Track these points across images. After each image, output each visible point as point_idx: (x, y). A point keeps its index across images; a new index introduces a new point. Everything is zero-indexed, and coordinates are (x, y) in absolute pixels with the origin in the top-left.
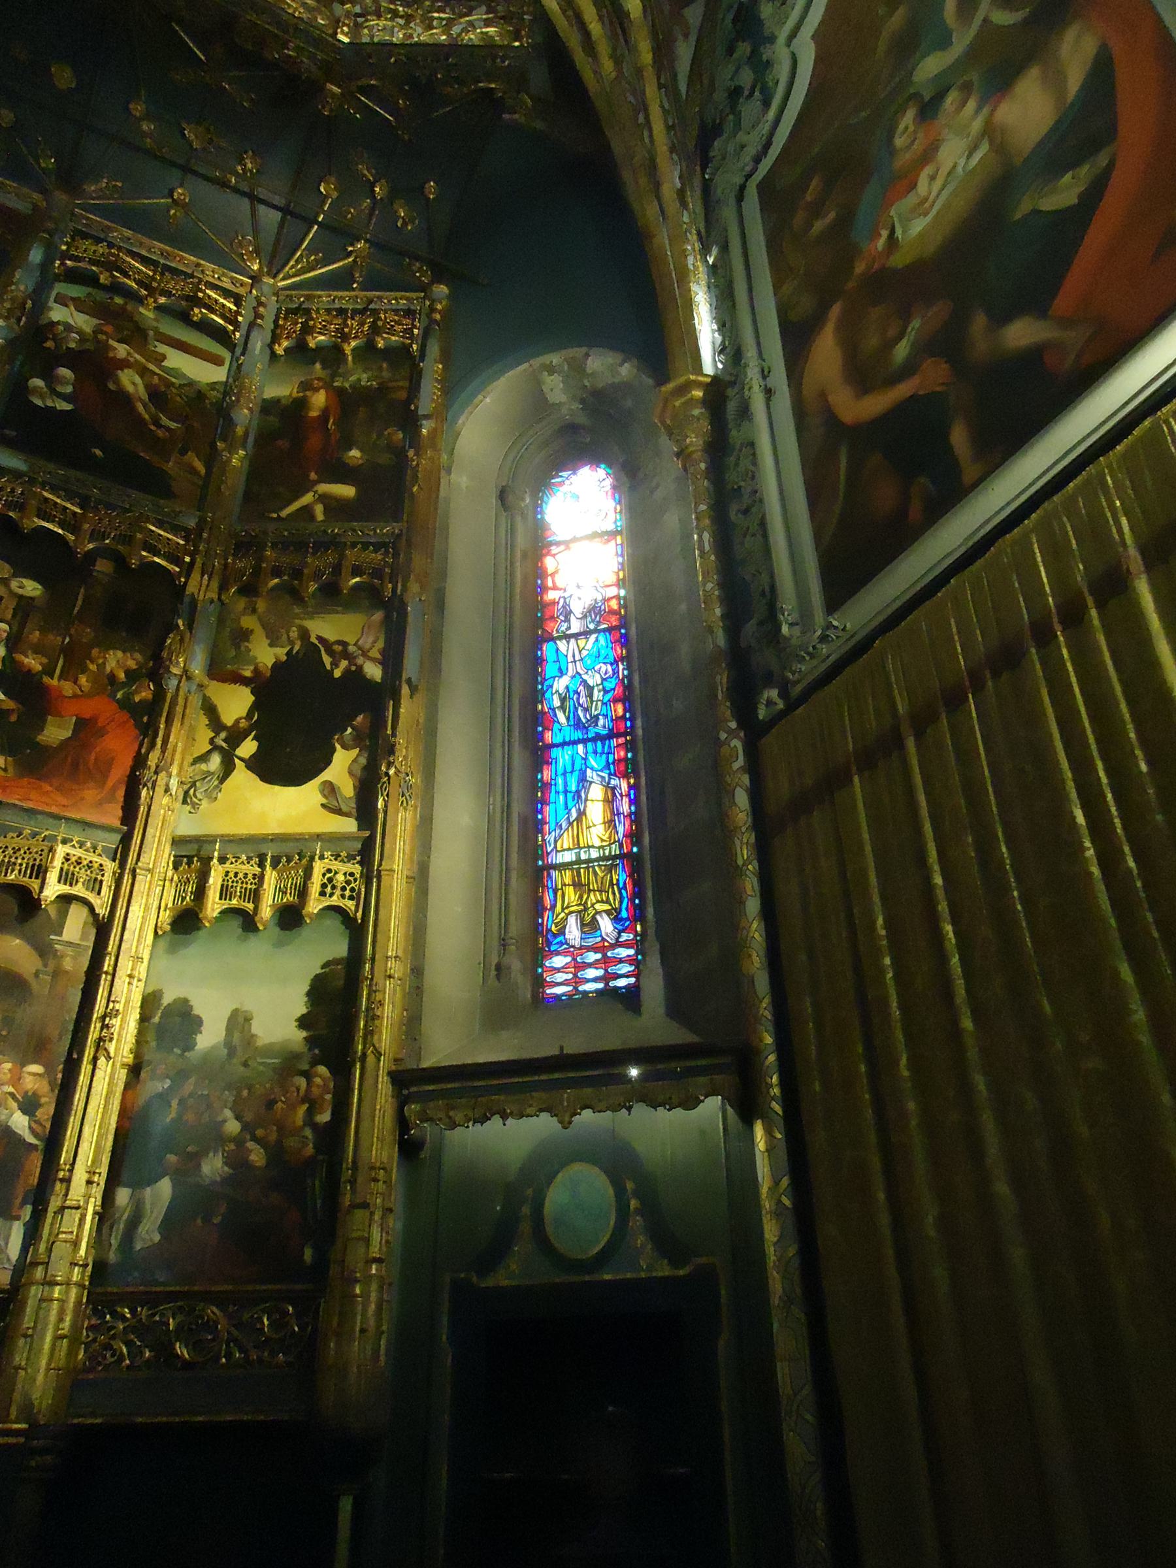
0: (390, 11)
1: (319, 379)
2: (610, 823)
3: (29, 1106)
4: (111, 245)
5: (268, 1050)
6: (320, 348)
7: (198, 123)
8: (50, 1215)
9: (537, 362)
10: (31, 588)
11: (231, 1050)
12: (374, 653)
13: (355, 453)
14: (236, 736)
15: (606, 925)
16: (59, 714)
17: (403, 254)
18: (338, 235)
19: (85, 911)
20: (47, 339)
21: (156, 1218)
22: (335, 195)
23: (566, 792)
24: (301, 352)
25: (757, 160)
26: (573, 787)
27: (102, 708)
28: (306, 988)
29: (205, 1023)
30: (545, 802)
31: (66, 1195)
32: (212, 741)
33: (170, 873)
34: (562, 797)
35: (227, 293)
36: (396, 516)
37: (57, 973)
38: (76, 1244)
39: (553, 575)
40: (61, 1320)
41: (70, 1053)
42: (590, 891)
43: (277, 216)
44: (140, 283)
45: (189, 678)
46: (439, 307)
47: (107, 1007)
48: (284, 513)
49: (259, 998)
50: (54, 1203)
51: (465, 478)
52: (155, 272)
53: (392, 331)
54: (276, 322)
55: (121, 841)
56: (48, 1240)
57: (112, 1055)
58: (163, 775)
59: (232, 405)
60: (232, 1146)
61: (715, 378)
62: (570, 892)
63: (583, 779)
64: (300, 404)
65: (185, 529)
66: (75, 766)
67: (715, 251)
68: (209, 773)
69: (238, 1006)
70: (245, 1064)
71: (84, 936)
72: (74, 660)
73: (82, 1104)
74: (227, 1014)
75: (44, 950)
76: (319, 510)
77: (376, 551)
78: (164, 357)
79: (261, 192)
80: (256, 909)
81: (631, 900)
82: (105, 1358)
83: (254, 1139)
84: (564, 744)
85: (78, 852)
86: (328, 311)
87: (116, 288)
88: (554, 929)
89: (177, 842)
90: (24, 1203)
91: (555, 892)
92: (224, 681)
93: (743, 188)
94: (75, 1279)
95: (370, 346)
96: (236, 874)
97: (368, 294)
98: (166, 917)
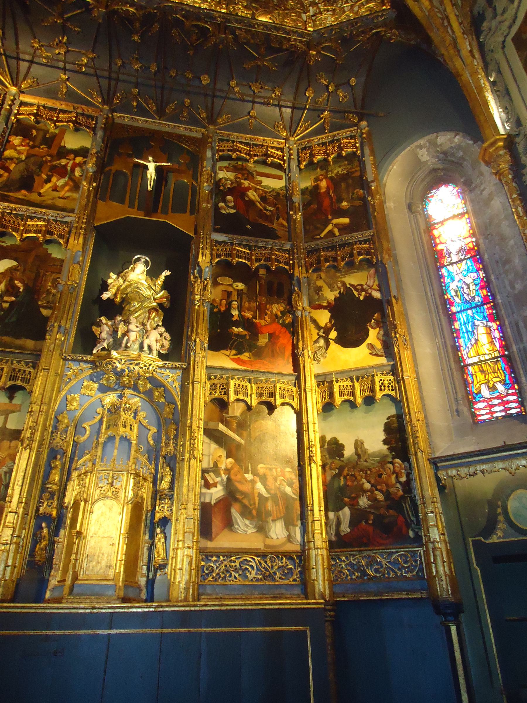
0: (325, 10)
1: (321, 175)
2: (492, 343)
4: (233, 142)
5: (374, 455)
6: (319, 162)
7: (256, 81)
9: (413, 146)
10: (240, 286)
11: (359, 456)
12: (375, 287)
13: (345, 203)
14: (327, 331)
15: (500, 388)
16: (262, 333)
17: (345, 112)
18: (317, 111)
19: (289, 408)
20: (220, 186)
22: (312, 95)
23: (467, 332)
24: (311, 165)
25: (510, 27)
26: (470, 329)
27: (276, 327)
28: (383, 428)
30: (458, 337)
32: (318, 334)
33: (317, 389)
34: (466, 334)
35: (277, 149)
36: (369, 228)
38: (322, 534)
39: (438, 238)
40: (323, 562)
43: (289, 110)
44: (246, 154)
45: (305, 310)
46: (364, 131)
48: (322, 235)
50: (310, 519)
51: (392, 204)
52: (250, 148)
53: (347, 147)
54: (298, 155)
55: (296, 379)
58: (306, 351)
59: (291, 196)
60: (369, 493)
61: (509, 135)
62: (479, 374)
63: (474, 325)
64: (317, 188)
65: (287, 250)
66: (272, 351)
67: (494, 75)
68: (320, 347)
70: (366, 461)
72: (262, 310)
76: (336, 231)
77: (365, 244)
78: (261, 182)
79: (282, 103)
81: (510, 375)
83: (377, 490)
84: (461, 311)
85: (283, 386)
86: (318, 145)
87: (239, 159)
88: (475, 391)
89: (317, 376)
91: (472, 375)
92: (316, 309)
93: (504, 42)
95: (339, 156)
97: (334, 133)
98: (320, 406)
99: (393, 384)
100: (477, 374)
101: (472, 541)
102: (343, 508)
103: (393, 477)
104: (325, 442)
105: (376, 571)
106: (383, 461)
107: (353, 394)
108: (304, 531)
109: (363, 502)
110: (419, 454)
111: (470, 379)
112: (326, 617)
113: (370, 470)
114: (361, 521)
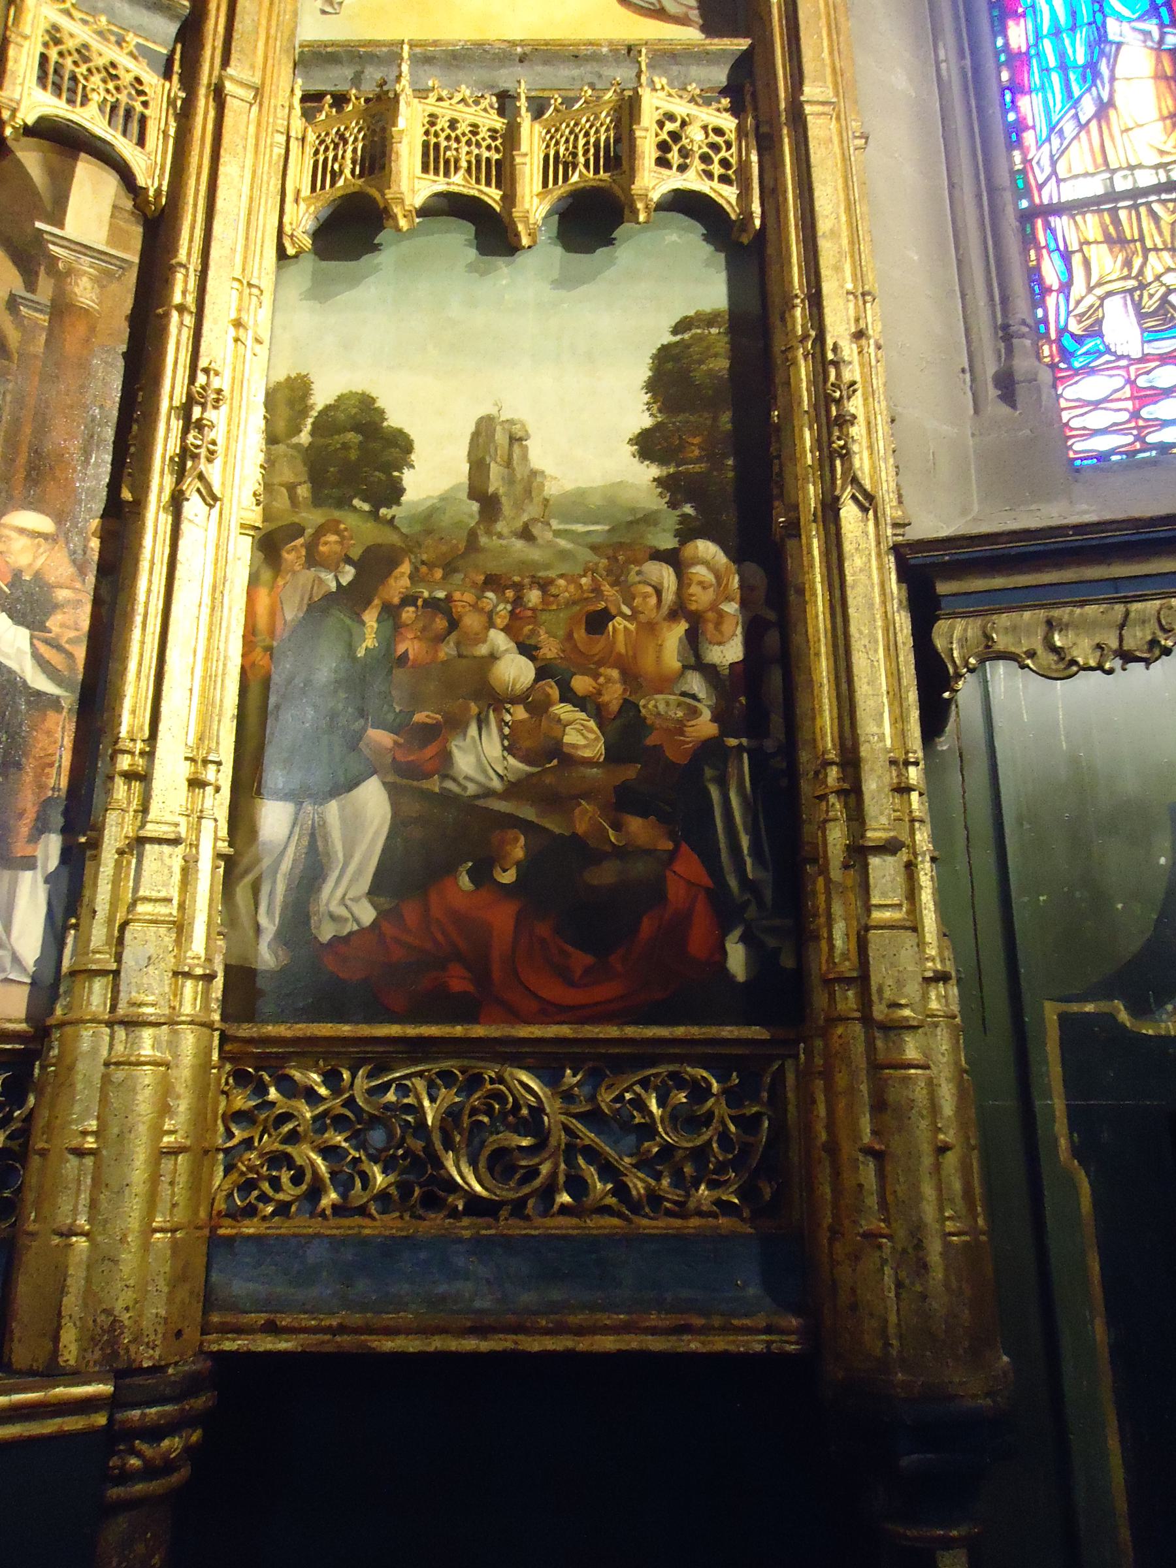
3: (28, 604)
5: (576, 506)
8: (108, 855)
11: (489, 505)
19: (110, 182)
21: (359, 871)
23: (1063, 67)
26: (1080, 55)
29: (416, 445)
30: (1017, 88)
31: (144, 809)
33: (297, 124)
34: (1056, 77)
37: (62, 309)
38: (180, 928)
40: (165, 1110)
41: (114, 487)
42: (1146, 251)
47: (192, 379)
49: (542, 389)
50: (116, 830)
55: (181, 36)
56: (110, 920)
57: (217, 490)
60: (520, 713)
70: (526, 534)
71: (115, 234)
73: (157, 605)
74: (472, 428)
80: (509, 199)
82: (275, 1184)
83: (568, 696)
88: (1075, 327)
90: (40, 829)
91: (1066, 257)
94: (187, 1009)
96: (453, 124)
98: (302, 219)
99: (732, 155)
100: (1092, 252)
101: (1063, 1018)
102: (353, 784)
103: (674, 635)
104: (304, 412)
105: (500, 1164)
106: (622, 545)
107: (503, 173)
108: (69, 903)
110: (849, 512)
111: (1051, 272)
112: (126, 1477)
113: (544, 586)
114: (450, 869)
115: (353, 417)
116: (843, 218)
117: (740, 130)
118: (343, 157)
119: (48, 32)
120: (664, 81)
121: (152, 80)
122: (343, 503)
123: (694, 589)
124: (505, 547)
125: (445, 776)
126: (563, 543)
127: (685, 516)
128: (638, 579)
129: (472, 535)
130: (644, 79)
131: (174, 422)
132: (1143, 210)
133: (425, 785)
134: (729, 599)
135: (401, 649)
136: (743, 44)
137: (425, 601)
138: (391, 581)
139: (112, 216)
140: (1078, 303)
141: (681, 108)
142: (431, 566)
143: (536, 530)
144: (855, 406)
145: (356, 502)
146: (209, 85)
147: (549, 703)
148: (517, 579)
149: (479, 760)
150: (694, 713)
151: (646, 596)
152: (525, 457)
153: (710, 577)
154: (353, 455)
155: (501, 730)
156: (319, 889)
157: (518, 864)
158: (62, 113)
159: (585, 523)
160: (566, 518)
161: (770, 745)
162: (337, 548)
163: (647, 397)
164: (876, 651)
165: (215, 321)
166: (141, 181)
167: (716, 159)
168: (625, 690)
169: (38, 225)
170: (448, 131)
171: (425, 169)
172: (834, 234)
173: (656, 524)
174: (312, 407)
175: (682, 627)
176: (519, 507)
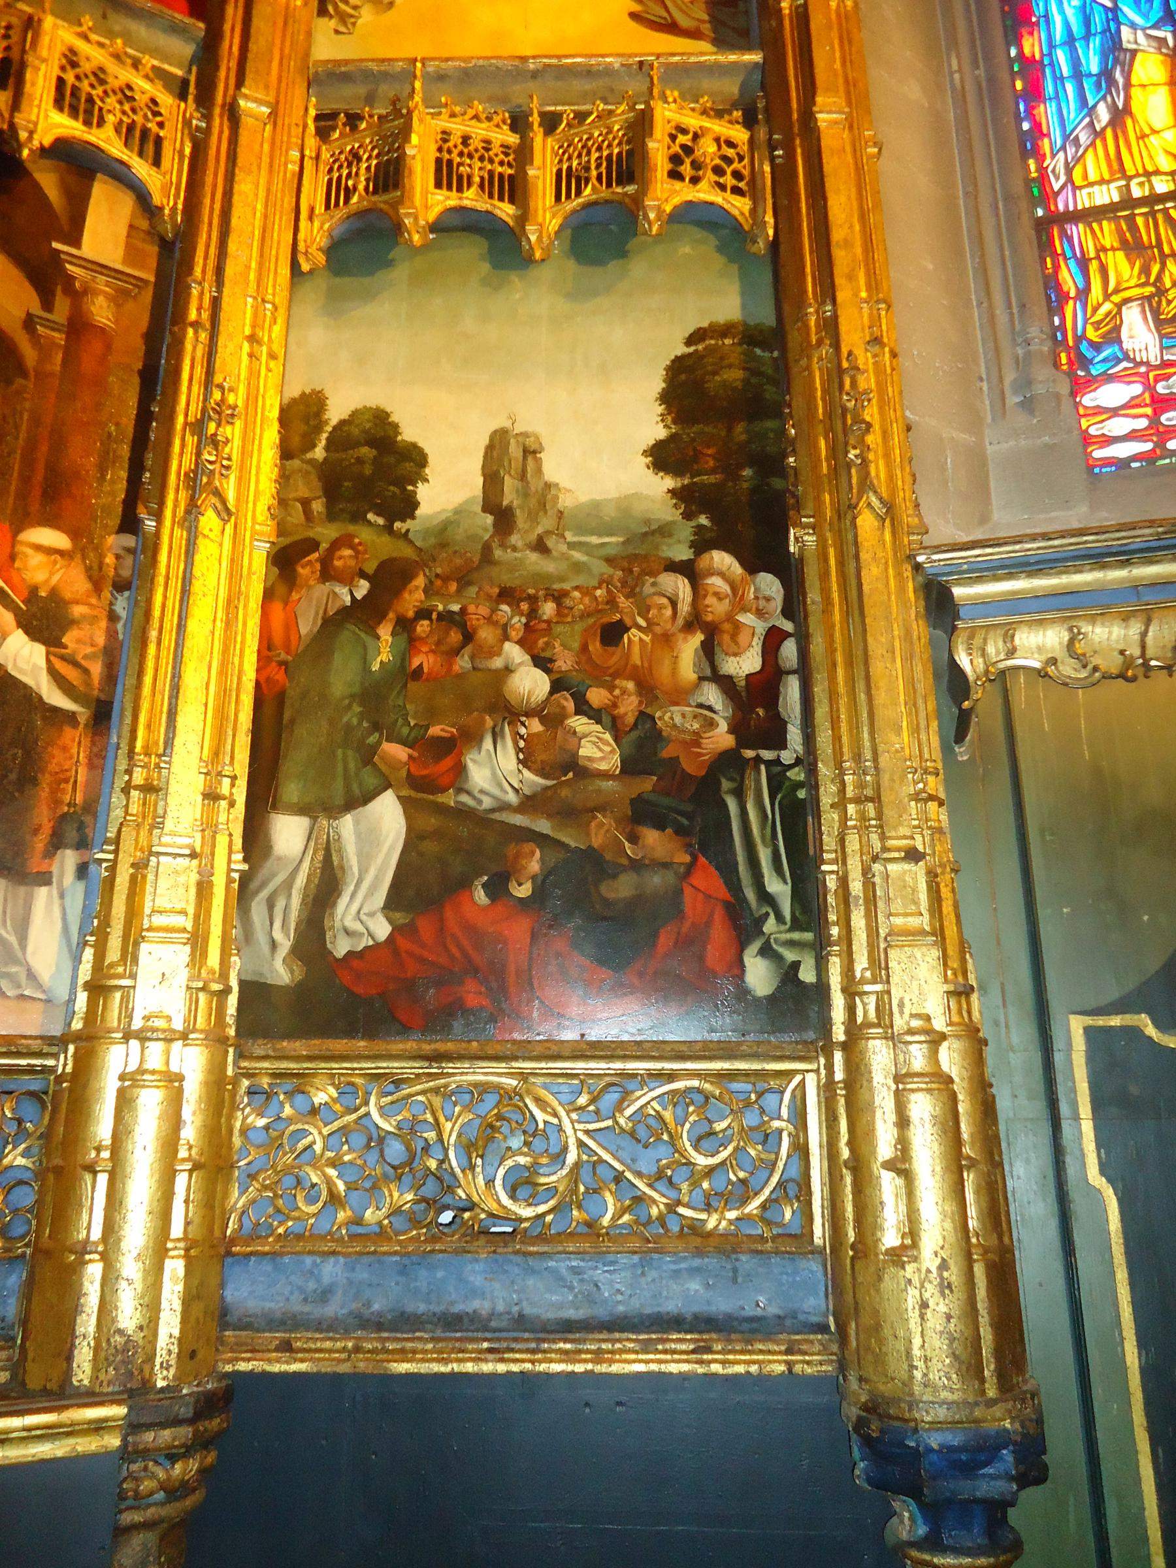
3: (44, 620)
5: (592, 518)
11: (504, 519)
19: (126, 204)
23: (1078, 75)
26: (1093, 64)
29: (430, 460)
33: (311, 142)
34: (1070, 87)
37: (79, 327)
42: (1164, 258)
60: (536, 726)
69: (507, 424)
70: (540, 546)
71: (132, 253)
73: (171, 621)
75: (46, 276)
83: (583, 707)
88: (1091, 334)
96: (466, 140)
98: (316, 233)
99: (743, 167)
100: (1110, 259)
101: (1087, 1030)
102: (367, 798)
104: (318, 429)
107: (514, 188)
109: (494, 772)
110: (866, 522)
111: (1069, 278)
113: (558, 597)
114: (465, 884)
115: (367, 432)
116: (857, 228)
117: (751, 141)
118: (357, 174)
119: (65, 56)
120: (676, 94)
121: (166, 101)
122: (358, 517)
123: (710, 600)
124: (520, 559)
125: (460, 790)
126: (577, 556)
127: (700, 527)
128: (652, 590)
129: (487, 549)
130: (656, 92)
131: (188, 437)
132: (1160, 217)
133: (441, 798)
134: (745, 610)
135: (416, 662)
136: (755, 57)
137: (439, 614)
138: (406, 595)
139: (128, 236)
140: (1095, 310)
141: (693, 122)
142: (446, 579)
143: (550, 542)
144: (871, 413)
145: (370, 516)
146: (223, 105)
147: (561, 717)
148: (531, 591)
149: (494, 774)
150: (711, 724)
151: (661, 607)
152: (539, 471)
153: (725, 588)
154: (368, 470)
155: (516, 744)
156: (334, 905)
157: (534, 878)
158: (77, 134)
159: (600, 535)
160: (581, 530)
161: (787, 757)
162: (352, 563)
163: (660, 409)
164: (894, 661)
165: (231, 337)
166: (157, 199)
167: (729, 171)
168: (640, 702)
169: (55, 245)
170: (460, 147)
171: (438, 185)
172: (847, 244)
173: (670, 535)
174: (326, 422)
175: (699, 637)
176: (533, 518)
